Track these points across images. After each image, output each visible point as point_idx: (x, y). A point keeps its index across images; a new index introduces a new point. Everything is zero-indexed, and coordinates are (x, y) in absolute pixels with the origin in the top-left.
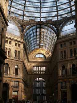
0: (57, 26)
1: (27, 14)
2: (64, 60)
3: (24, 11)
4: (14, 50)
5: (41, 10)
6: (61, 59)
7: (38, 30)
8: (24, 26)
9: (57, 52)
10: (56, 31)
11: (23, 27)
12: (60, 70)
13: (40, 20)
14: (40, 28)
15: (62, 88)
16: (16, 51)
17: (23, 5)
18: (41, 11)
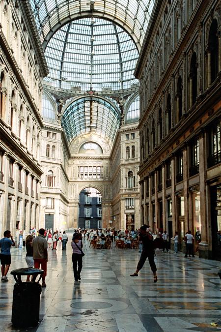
0: (120, 101)
1: (69, 77)
2: (130, 162)
3: (61, 72)
4: (46, 145)
5: (92, 68)
6: (126, 160)
7: (87, 104)
8: (61, 101)
9: (120, 148)
10: (119, 109)
11: (60, 102)
12: (125, 179)
13: (91, 88)
14: (91, 102)
15: (127, 208)
16: (48, 145)
17: (59, 61)
18: (91, 70)
